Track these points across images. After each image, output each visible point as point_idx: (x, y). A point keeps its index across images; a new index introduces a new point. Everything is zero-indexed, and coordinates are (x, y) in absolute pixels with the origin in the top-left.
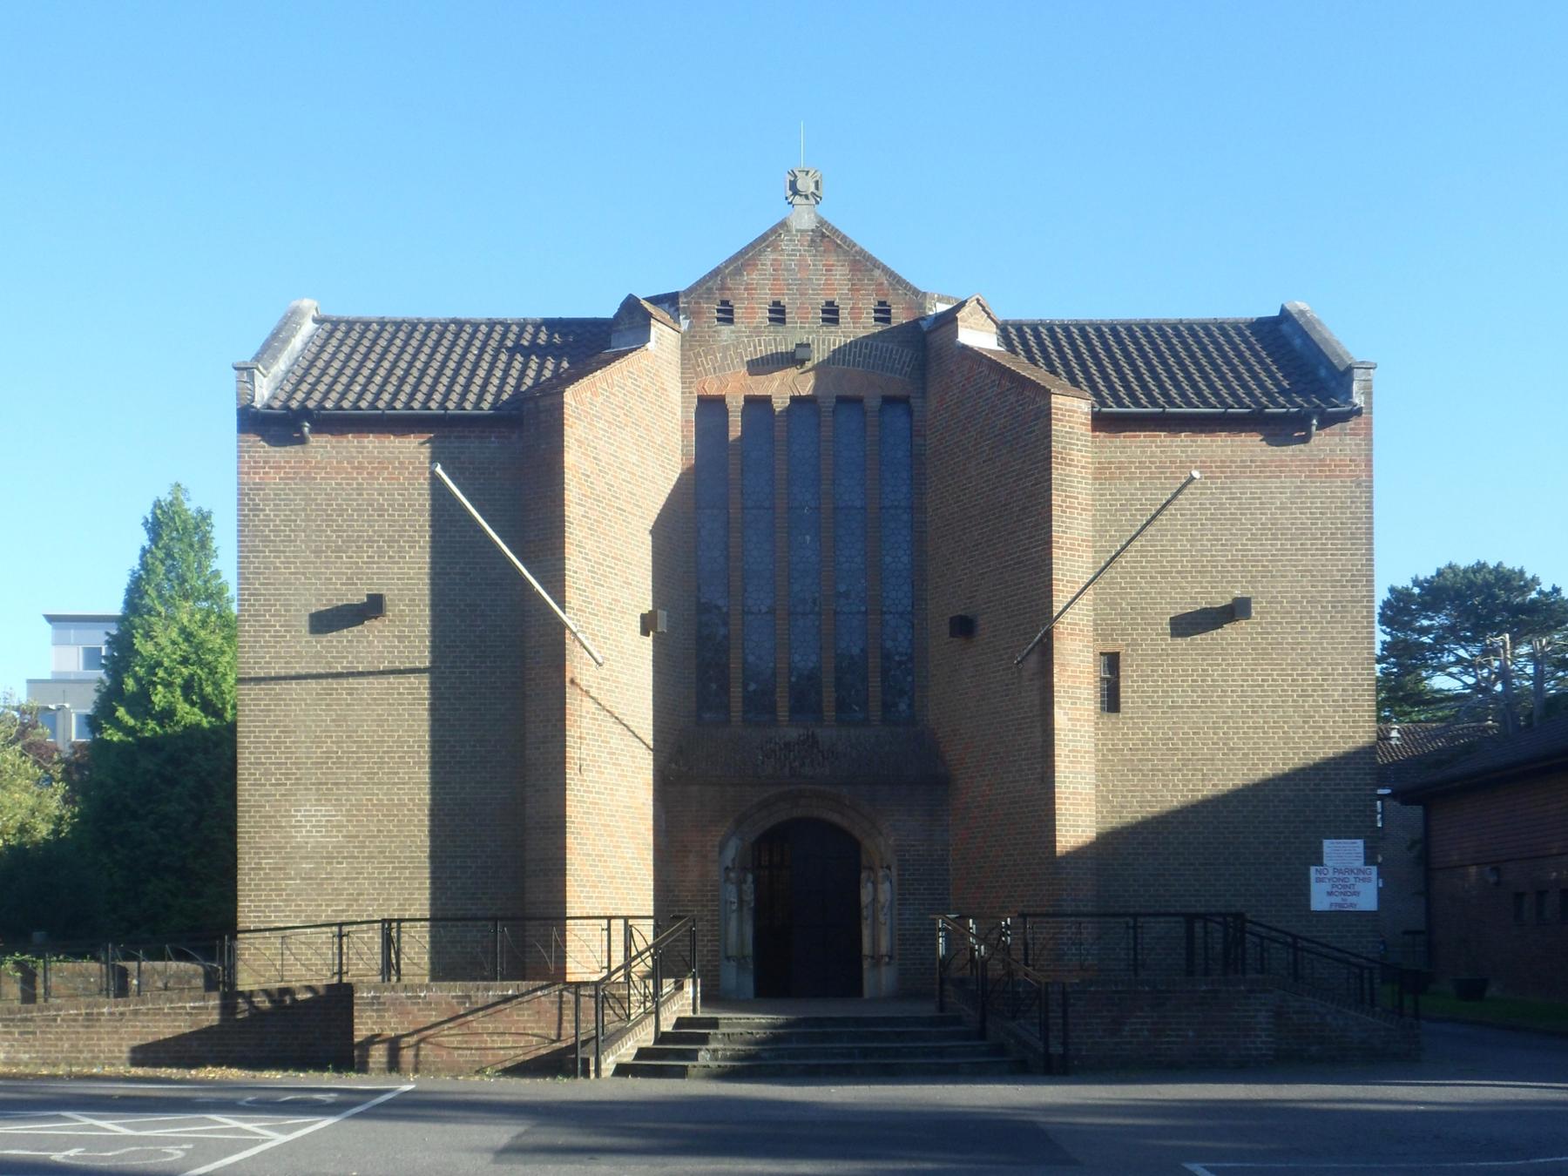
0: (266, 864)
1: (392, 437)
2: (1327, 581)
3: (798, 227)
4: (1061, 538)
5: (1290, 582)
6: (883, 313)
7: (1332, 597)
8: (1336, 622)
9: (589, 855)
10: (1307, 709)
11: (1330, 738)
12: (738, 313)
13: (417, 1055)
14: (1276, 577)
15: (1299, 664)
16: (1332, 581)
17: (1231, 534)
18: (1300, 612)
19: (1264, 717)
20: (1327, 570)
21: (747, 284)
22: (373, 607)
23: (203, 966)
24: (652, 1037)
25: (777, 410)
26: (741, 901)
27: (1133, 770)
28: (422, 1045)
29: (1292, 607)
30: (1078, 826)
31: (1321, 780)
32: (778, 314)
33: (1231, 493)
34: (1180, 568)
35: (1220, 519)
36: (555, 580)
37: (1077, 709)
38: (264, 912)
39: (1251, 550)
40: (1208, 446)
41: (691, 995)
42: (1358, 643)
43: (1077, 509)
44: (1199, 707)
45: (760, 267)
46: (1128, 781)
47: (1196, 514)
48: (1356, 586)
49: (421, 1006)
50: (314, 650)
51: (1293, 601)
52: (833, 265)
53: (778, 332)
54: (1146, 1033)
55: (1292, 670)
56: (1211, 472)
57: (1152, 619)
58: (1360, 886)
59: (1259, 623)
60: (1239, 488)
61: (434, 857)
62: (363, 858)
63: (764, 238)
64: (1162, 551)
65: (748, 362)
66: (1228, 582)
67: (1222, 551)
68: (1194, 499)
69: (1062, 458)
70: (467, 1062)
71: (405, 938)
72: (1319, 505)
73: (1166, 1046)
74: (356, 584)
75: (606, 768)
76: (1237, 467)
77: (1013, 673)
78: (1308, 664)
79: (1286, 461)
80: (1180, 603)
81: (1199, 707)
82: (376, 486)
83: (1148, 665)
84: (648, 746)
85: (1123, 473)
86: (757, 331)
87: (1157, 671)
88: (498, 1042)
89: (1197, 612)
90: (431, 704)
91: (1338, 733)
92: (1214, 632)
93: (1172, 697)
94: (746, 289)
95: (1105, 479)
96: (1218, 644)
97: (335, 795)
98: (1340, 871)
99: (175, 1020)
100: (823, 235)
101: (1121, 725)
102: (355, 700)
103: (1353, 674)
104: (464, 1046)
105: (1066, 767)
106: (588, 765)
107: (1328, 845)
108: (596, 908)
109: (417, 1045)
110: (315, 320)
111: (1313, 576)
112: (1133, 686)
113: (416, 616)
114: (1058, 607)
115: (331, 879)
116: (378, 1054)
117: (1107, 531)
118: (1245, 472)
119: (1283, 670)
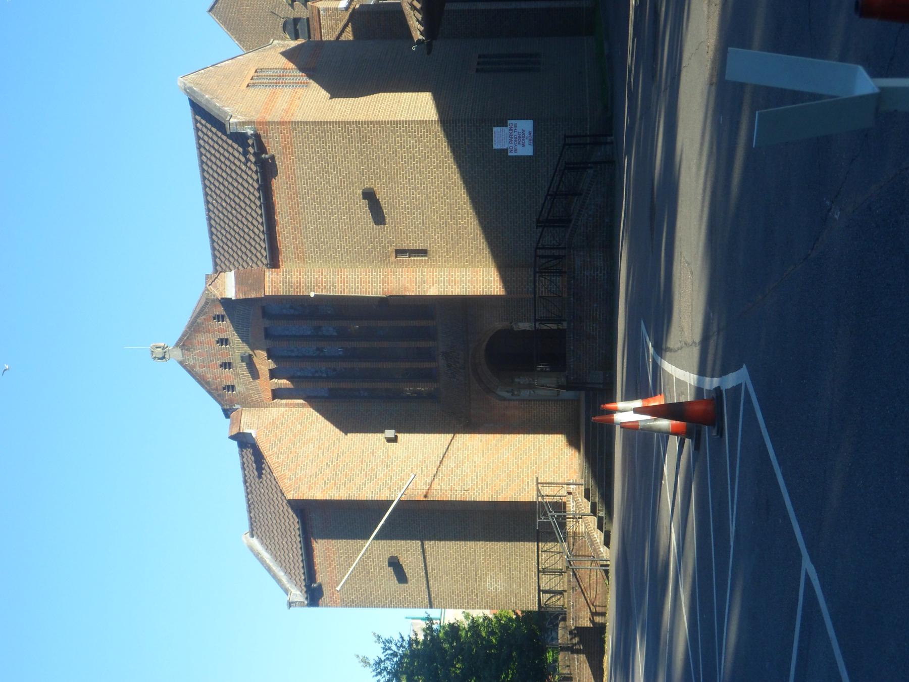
0: (513, 600)
1: (314, 553)
2: (349, 146)
3: (181, 356)
5: (351, 165)
6: (220, 318)
7: (358, 143)
8: (372, 141)
10: (420, 157)
11: (436, 144)
12: (228, 383)
13: (599, 606)
14: (349, 171)
15: (396, 160)
16: (349, 143)
17: (328, 194)
18: (368, 159)
19: (427, 178)
20: (344, 145)
21: (213, 379)
22: (395, 564)
23: (560, 621)
25: (275, 366)
27: (458, 243)
28: (595, 604)
29: (365, 164)
30: (489, 279)
32: (227, 365)
33: (305, 194)
34: (348, 220)
35: (320, 200)
39: (336, 185)
40: (281, 205)
42: (383, 129)
44: (423, 211)
45: (204, 374)
46: (463, 246)
47: (319, 212)
48: (351, 130)
49: (577, 604)
50: (415, 582)
51: (362, 163)
52: (198, 341)
53: (236, 366)
54: (594, 325)
55: (400, 164)
56: (295, 204)
57: (376, 233)
58: (519, 129)
59: (375, 180)
60: (302, 190)
61: (510, 540)
62: (510, 565)
63: (189, 372)
64: (339, 228)
65: (253, 379)
66: (354, 196)
67: (337, 199)
68: (310, 213)
70: (602, 589)
72: (308, 149)
73: (601, 316)
74: (383, 567)
76: (291, 191)
78: (396, 156)
79: (285, 166)
80: (367, 220)
81: (423, 211)
82: (338, 559)
83: (401, 236)
84: (453, 438)
85: (300, 247)
86: (237, 375)
87: (404, 231)
88: (594, 578)
89: (371, 212)
90: (438, 540)
91: (433, 140)
92: (381, 203)
93: (418, 224)
94: (216, 380)
95: (303, 255)
96: (388, 201)
97: (481, 575)
98: (511, 140)
99: (583, 669)
100: (183, 345)
101: (434, 249)
102: (437, 568)
104: (595, 589)
109: (595, 607)
111: (347, 153)
112: (413, 243)
113: (396, 545)
115: (520, 577)
116: (598, 619)
117: (331, 255)
118: (293, 187)
119: (400, 169)
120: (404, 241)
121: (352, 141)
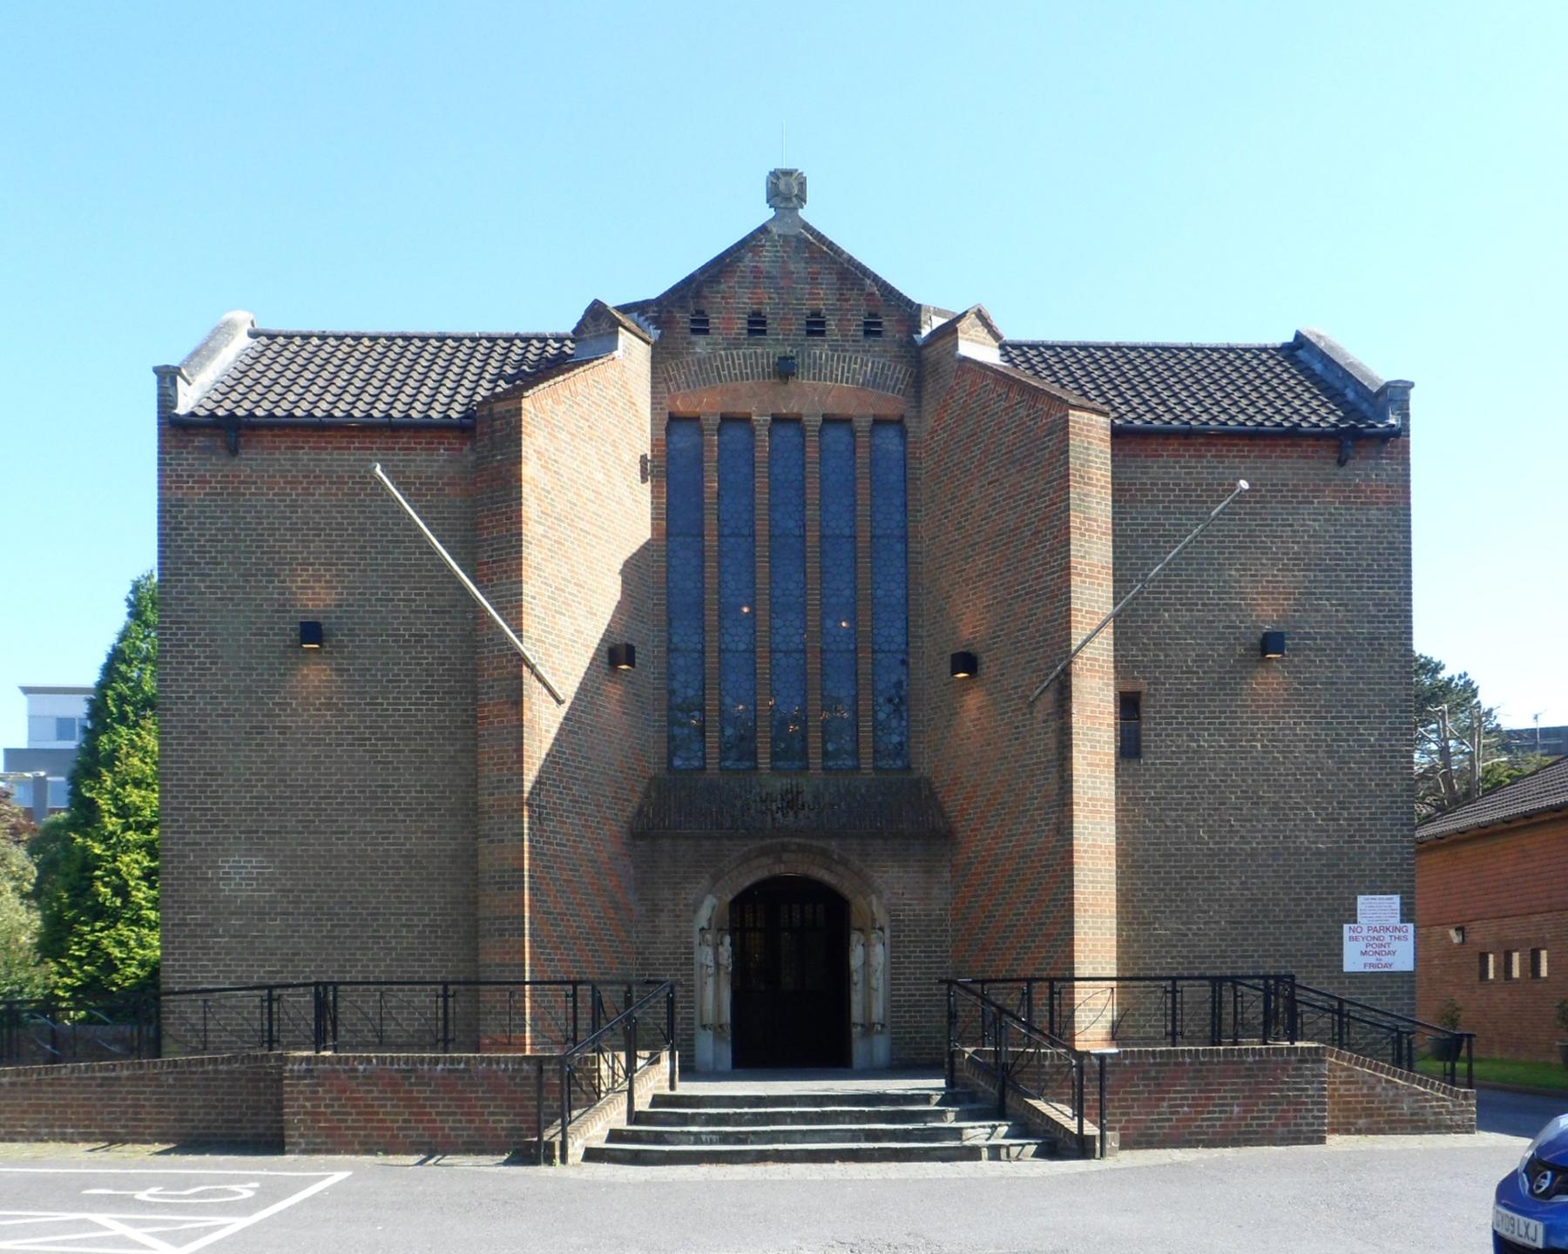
4: (1080, 563)
9: (550, 913)
12: (714, 321)
18: (1335, 649)
24: (624, 1116)
26: (718, 964)
30: (1097, 882)
31: (1356, 831)
36: (512, 606)
37: (1097, 754)
38: (189, 972)
41: (668, 1070)
43: (1096, 532)
52: (819, 273)
58: (1395, 945)
69: (1081, 476)
71: (342, 1004)
75: (568, 817)
77: (1024, 714)
98: (1375, 930)
103: (1390, 717)
105: (1085, 817)
106: (548, 814)
107: (1363, 902)
108: (559, 972)
110: (254, 335)
114: (1080, 634)
120: (1159, 712)
121: (1373, 622)
